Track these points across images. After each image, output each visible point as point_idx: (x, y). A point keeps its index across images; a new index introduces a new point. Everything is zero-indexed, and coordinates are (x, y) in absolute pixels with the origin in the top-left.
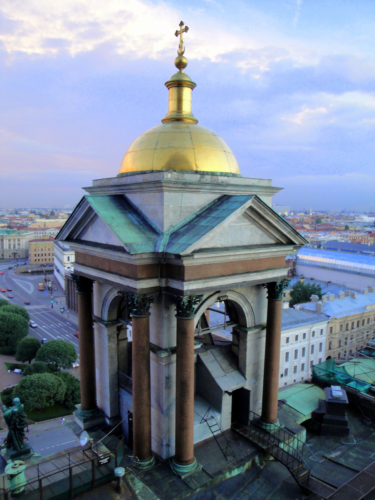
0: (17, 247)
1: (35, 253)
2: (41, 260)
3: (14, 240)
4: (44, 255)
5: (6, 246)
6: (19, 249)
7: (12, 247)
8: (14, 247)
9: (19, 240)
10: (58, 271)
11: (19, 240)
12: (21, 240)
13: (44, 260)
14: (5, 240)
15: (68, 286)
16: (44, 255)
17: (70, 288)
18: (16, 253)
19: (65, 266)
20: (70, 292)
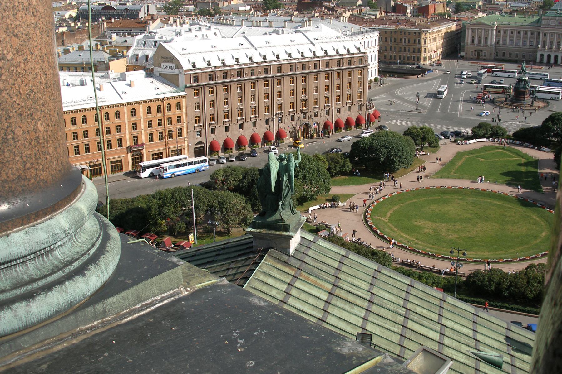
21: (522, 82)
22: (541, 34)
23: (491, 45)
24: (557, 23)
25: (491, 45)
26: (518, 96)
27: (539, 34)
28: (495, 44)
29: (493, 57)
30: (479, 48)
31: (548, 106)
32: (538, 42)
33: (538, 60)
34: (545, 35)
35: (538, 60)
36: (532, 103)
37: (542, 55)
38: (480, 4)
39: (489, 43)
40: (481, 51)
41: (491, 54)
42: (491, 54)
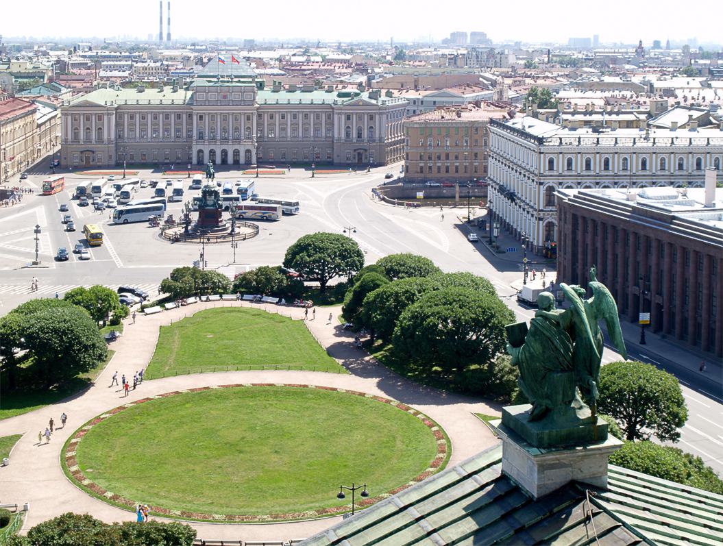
0: (365, 134)
1: (421, 150)
2: (435, 170)
3: (360, 118)
4: (443, 157)
5: (339, 132)
6: (371, 139)
7: (354, 134)
8: (359, 136)
9: (371, 118)
10: (511, 196)
11: (371, 118)
12: (377, 117)
13: (443, 170)
14: (336, 117)
15: (574, 232)
16: (443, 157)
17: (579, 237)
18: (366, 150)
19: (541, 184)
20: (580, 250)
21: (210, 195)
22: (195, 117)
23: (109, 141)
24: (220, 98)
25: (109, 141)
26: (208, 219)
27: (190, 116)
28: (116, 139)
29: (113, 162)
30: (89, 147)
31: (258, 233)
32: (189, 131)
33: (194, 161)
34: (201, 117)
35: (194, 161)
36: (233, 230)
37: (200, 151)
38: (50, 74)
39: (105, 137)
40: (93, 152)
41: (110, 157)
42: (110, 157)
